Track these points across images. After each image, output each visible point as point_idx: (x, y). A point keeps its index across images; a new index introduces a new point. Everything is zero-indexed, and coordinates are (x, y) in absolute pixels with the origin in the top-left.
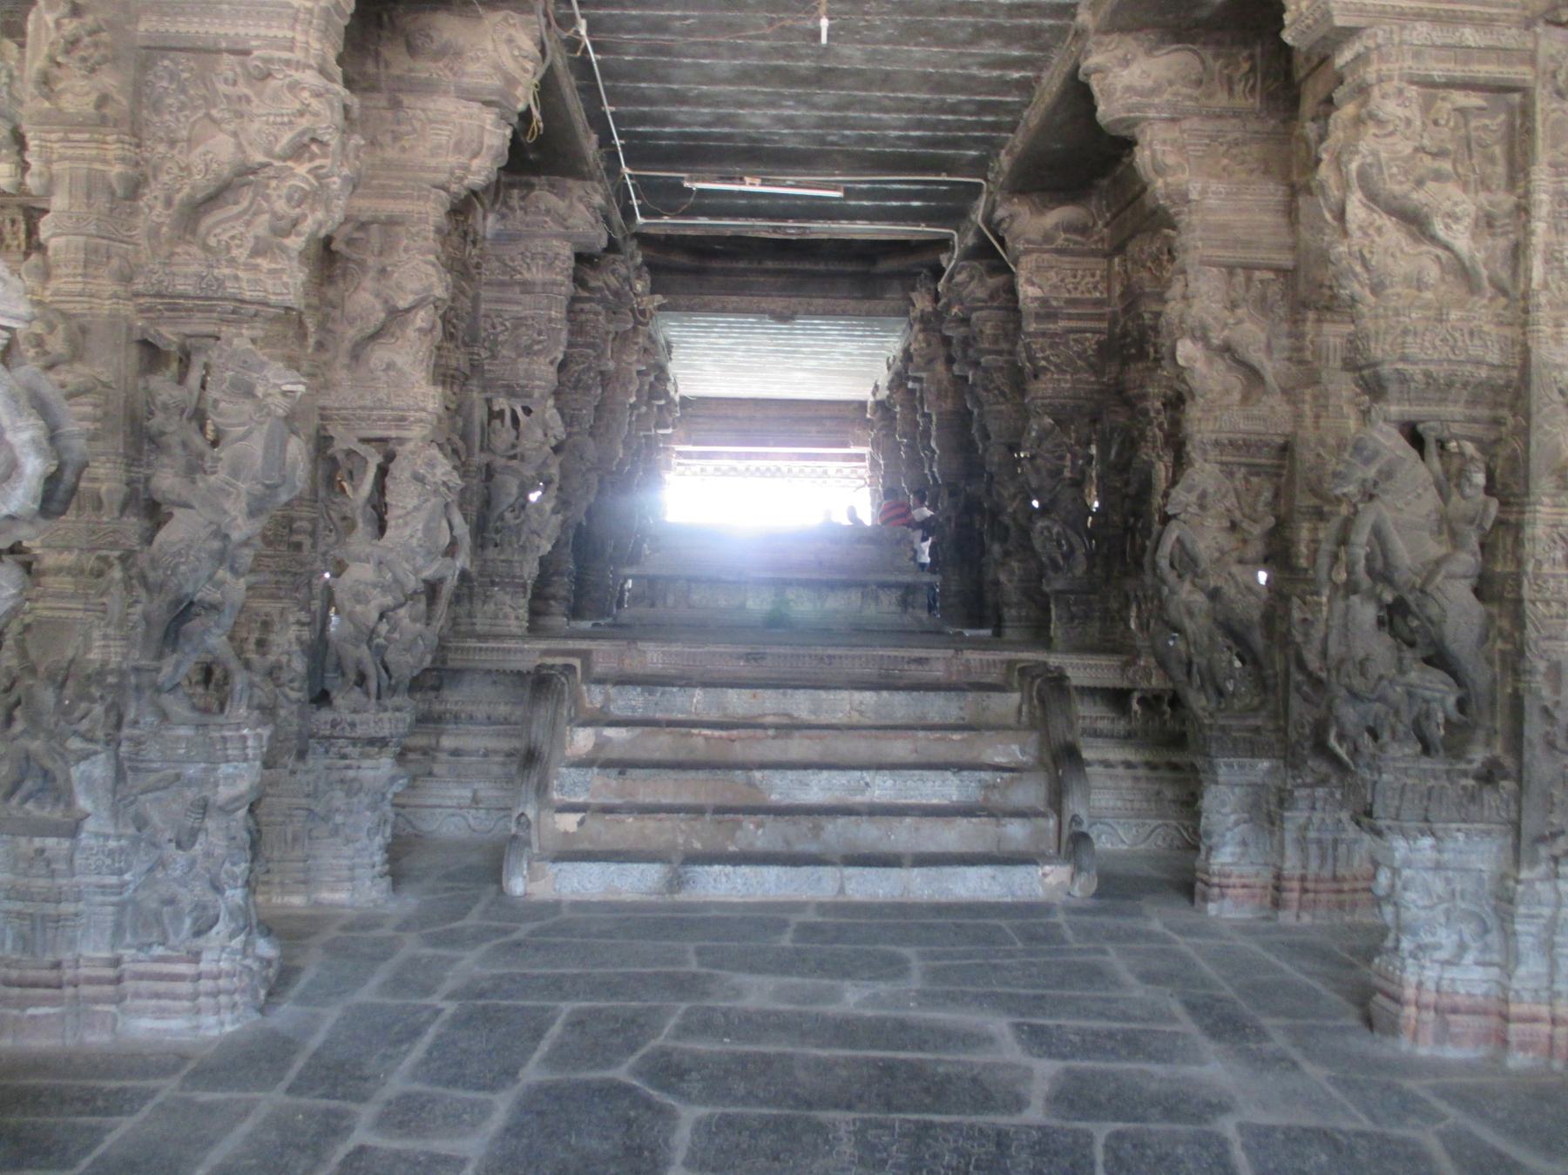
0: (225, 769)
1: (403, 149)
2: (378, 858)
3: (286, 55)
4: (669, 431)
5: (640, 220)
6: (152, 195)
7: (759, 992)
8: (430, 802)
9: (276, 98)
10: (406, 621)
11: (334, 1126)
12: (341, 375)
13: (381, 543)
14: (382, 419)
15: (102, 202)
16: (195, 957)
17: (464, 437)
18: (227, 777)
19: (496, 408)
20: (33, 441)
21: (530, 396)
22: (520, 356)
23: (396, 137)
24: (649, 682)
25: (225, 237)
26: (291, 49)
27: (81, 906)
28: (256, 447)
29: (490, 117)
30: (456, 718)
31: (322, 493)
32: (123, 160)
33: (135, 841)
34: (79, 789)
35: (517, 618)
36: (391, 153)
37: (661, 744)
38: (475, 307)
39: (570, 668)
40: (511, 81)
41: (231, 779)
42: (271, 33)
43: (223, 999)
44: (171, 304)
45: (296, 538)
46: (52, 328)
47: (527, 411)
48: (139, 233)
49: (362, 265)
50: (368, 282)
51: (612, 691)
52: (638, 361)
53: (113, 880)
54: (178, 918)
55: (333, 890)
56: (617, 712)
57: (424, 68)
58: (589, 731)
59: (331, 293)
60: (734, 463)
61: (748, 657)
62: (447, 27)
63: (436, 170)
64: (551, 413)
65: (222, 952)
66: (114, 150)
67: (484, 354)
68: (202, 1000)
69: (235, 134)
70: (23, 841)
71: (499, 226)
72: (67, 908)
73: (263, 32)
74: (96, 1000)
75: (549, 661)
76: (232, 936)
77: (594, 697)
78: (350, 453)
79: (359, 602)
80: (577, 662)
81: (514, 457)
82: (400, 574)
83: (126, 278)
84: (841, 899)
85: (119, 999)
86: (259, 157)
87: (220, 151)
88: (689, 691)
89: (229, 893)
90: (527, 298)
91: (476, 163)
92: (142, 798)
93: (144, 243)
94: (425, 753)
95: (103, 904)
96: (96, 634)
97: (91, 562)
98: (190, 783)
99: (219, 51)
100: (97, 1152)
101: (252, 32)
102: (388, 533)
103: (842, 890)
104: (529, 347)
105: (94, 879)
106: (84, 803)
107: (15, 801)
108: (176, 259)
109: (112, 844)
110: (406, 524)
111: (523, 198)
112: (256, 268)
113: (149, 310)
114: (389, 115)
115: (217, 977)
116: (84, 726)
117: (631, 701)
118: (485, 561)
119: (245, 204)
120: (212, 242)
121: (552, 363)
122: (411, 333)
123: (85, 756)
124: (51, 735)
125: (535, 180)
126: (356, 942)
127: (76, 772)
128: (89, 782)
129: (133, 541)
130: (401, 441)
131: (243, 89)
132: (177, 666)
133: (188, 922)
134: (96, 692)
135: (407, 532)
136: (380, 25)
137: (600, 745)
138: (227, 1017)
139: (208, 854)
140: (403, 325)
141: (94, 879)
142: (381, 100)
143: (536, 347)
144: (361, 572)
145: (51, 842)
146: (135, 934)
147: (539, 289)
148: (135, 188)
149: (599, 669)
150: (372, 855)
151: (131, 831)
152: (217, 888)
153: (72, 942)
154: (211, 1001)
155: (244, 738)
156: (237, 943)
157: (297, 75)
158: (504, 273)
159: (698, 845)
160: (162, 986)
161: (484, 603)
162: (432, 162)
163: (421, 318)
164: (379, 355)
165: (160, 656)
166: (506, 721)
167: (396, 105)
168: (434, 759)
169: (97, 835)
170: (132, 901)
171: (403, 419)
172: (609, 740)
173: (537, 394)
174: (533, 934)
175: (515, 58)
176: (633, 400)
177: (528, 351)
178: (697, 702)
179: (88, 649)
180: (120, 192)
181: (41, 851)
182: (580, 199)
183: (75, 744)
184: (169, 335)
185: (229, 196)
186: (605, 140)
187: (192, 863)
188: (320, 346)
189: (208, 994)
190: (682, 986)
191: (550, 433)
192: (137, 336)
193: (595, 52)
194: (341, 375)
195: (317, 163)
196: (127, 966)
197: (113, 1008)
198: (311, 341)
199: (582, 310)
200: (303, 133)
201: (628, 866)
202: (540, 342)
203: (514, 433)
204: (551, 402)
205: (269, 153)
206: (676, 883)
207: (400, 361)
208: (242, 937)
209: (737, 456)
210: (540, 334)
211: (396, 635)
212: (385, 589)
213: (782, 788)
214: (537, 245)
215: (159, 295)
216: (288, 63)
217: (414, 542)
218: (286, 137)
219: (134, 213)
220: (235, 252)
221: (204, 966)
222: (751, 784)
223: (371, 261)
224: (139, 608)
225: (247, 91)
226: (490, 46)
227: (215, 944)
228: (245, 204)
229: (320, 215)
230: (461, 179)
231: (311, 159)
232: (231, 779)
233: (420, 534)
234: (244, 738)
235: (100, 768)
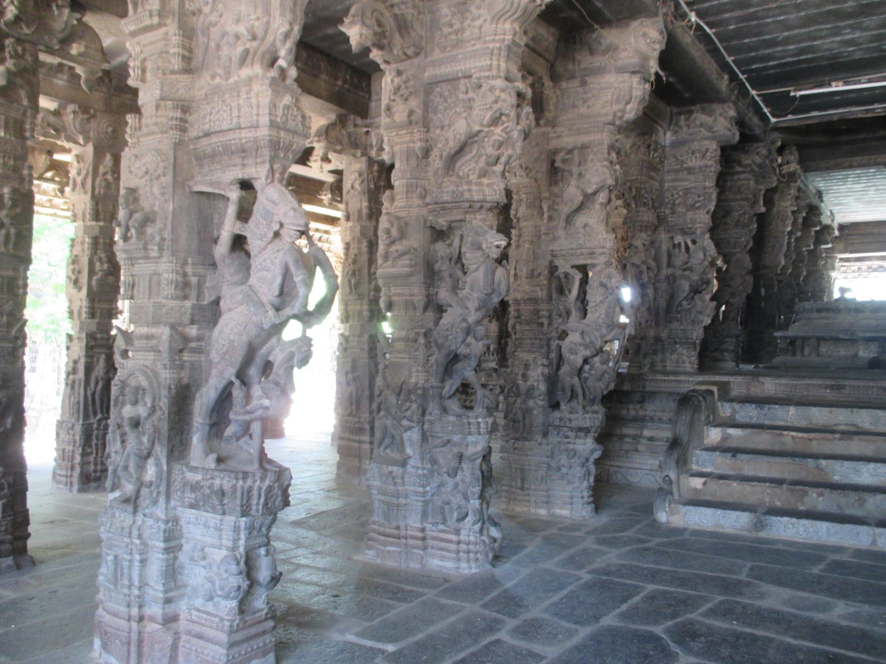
0: (471, 438)
1: (589, 107)
2: (585, 494)
3: (487, 74)
4: (830, 246)
5: (773, 120)
6: (435, 154)
7: (775, 598)
8: (634, 466)
9: (484, 96)
10: (598, 365)
11: (492, 626)
12: (561, 232)
13: (586, 321)
14: (582, 254)
15: (413, 162)
16: (457, 532)
17: (656, 259)
18: (473, 442)
19: (676, 242)
20: (303, 280)
21: (694, 233)
22: (688, 211)
23: (585, 101)
24: (761, 401)
25: (466, 170)
26: (490, 70)
27: (409, 501)
28: (481, 274)
29: (636, 79)
30: (652, 420)
31: (554, 296)
32: (420, 140)
33: (432, 472)
34: (407, 444)
35: (690, 363)
36: (583, 110)
37: (763, 440)
38: (662, 186)
39: (711, 393)
40: (645, 58)
41: (475, 443)
42: (481, 64)
44: (443, 207)
45: (541, 320)
46: (392, 224)
47: (694, 242)
48: (430, 174)
49: (570, 172)
50: (573, 182)
51: (737, 406)
52: (792, 205)
53: (421, 489)
55: (562, 508)
56: (740, 419)
57: (598, 61)
58: (718, 430)
59: (556, 189)
61: (832, 387)
62: (610, 36)
63: (606, 115)
64: (707, 242)
65: (469, 530)
66: (417, 136)
67: (668, 212)
68: (461, 554)
69: (466, 118)
70: (385, 467)
71: (674, 138)
72: (402, 501)
73: (477, 64)
74: (414, 547)
75: (698, 387)
76: (474, 524)
77: (725, 410)
78: (566, 275)
79: (572, 354)
80: (715, 389)
81: (685, 270)
83: (423, 197)
84: (874, 548)
85: (425, 548)
86: (477, 128)
87: (461, 128)
88: (786, 408)
89: (472, 501)
90: (691, 177)
91: (629, 107)
92: (435, 450)
93: (432, 178)
94: (634, 438)
95: (417, 501)
96: (414, 370)
97: (412, 335)
98: (455, 445)
99: (459, 79)
100: (385, 617)
101: (472, 66)
102: (588, 316)
103: (874, 542)
104: (694, 204)
105: (413, 488)
106: (409, 451)
107: (382, 448)
108: (444, 184)
109: (420, 472)
110: (596, 311)
111: (687, 120)
112: (480, 184)
113: (434, 211)
114: (580, 90)
115: (469, 543)
116: (408, 413)
117: (749, 413)
118: (671, 330)
119: (474, 152)
120: (461, 173)
121: (708, 213)
122: (597, 206)
123: (410, 428)
124: (394, 418)
125: (693, 108)
126: (557, 536)
127: (406, 435)
128: (410, 439)
129: (431, 325)
130: (594, 266)
132: (451, 387)
133: (456, 514)
134: (413, 397)
135: (597, 315)
136: (575, 43)
137: (724, 439)
138: (473, 565)
139: (463, 481)
140: (593, 202)
141: (413, 488)
142: (576, 83)
143: (697, 205)
144: (574, 337)
145: (395, 468)
146: (433, 517)
147: (697, 171)
148: (427, 152)
149: (735, 392)
150: (582, 492)
151: (429, 466)
152: (467, 499)
153: (405, 518)
154: (465, 555)
155: (479, 423)
156: (477, 527)
158: (677, 165)
159: (778, 504)
160: (443, 545)
161: (671, 354)
162: (604, 111)
163: (602, 197)
164: (580, 220)
165: (443, 381)
167: (584, 83)
168: (639, 442)
169: (414, 467)
170: (431, 501)
171: (593, 253)
172: (730, 436)
173: (699, 232)
174: (659, 545)
175: (648, 44)
176: (789, 229)
177: (693, 207)
178: (791, 414)
179: (410, 376)
180: (420, 156)
181: (391, 473)
182: (721, 115)
183: (405, 422)
184: (442, 222)
185: (467, 149)
186: (733, 77)
187: (456, 485)
188: (551, 218)
189: (464, 552)
190: (729, 586)
191: (707, 254)
192: (428, 224)
193: (711, 27)
194: (561, 232)
195: (505, 125)
196: (429, 533)
197: (422, 552)
198: (546, 216)
199: (739, 179)
200: (495, 112)
201: (729, 512)
202: (699, 201)
203: (686, 256)
204: (707, 236)
205: (481, 125)
206: (759, 525)
207: (591, 222)
208: (479, 525)
210: (699, 196)
212: (586, 347)
213: (841, 472)
214: (696, 145)
215: (437, 203)
216: (488, 77)
217: (600, 321)
218: (488, 116)
219: (428, 164)
220: (471, 177)
221: (462, 537)
222: (818, 468)
223: (575, 170)
224: (434, 357)
226: (632, 40)
227: (467, 527)
228: (474, 152)
229: (510, 152)
230: (621, 118)
231: (503, 124)
232: (475, 443)
233: (603, 316)
234: (479, 423)
235: (414, 435)
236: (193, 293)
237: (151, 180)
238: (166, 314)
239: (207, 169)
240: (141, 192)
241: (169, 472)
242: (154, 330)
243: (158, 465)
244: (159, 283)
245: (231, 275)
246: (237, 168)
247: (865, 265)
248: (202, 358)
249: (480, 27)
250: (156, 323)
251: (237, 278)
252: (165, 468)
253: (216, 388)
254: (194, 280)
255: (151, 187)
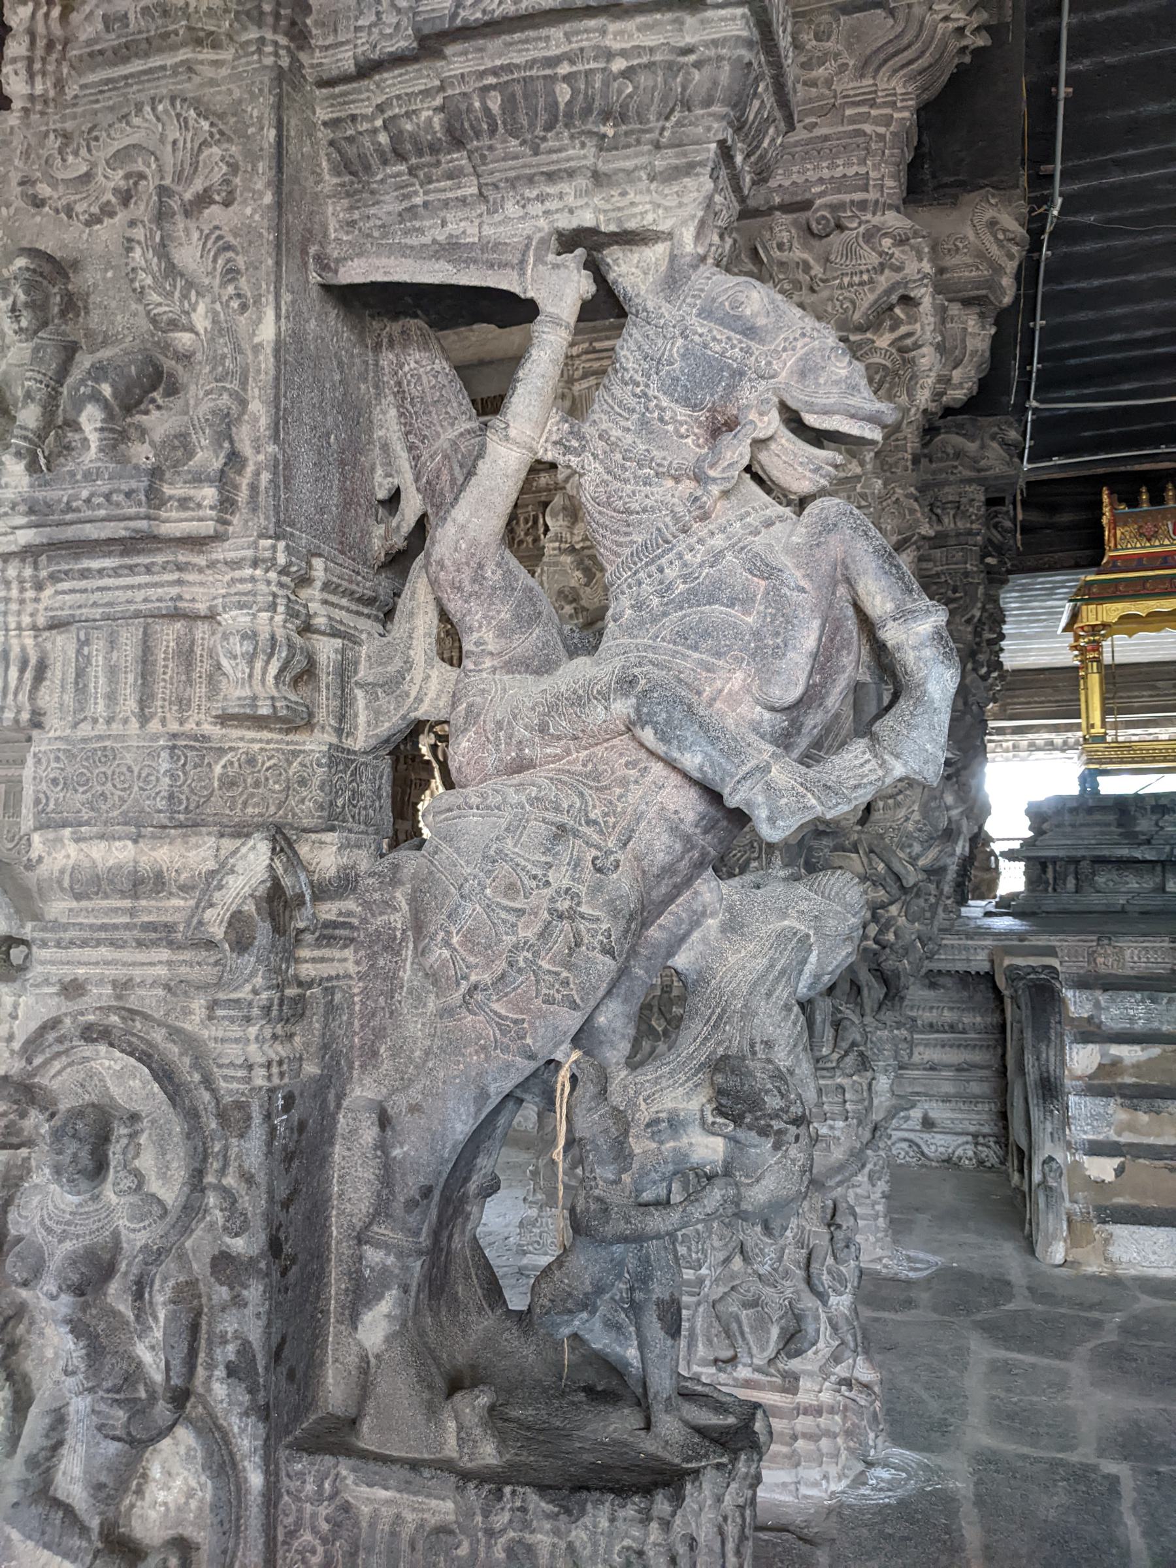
3: (858, 196)
10: (902, 921)
16: (790, 1383)
20: (937, 635)
42: (838, 172)
43: (824, 1443)
51: (1103, 998)
54: (761, 1325)
56: (1110, 1024)
60: (1052, 736)
68: (800, 1443)
73: (826, 173)
82: (897, 867)
89: (833, 1300)
90: (937, 553)
91: (957, 375)
99: (771, 210)
101: (812, 175)
110: (898, 805)
115: (818, 1411)
131: (798, 254)
133: (775, 1332)
137: (1111, 1067)
147: (952, 541)
154: (811, 1446)
157: (877, 220)
166: (952, 1028)
195: (903, 330)
200: (889, 292)
209: (1056, 729)
210: (955, 591)
211: (891, 937)
216: (863, 205)
217: (910, 826)
218: (868, 298)
221: (803, 1398)
225: (806, 256)
231: (893, 329)
233: (916, 816)
234: (842, 1089)
236: (325, 702)
237: (162, 215)
238: (229, 783)
239: (391, 205)
240: (90, 277)
241: (271, 1496)
242: (162, 855)
243: (222, 1464)
244: (186, 655)
245: (503, 632)
246: (565, 187)
247: (1024, 740)
248: (345, 962)
249: (829, 83)
250: (186, 821)
251: (528, 642)
252: (255, 1480)
253: (483, 1095)
254: (326, 650)
255: (162, 251)
